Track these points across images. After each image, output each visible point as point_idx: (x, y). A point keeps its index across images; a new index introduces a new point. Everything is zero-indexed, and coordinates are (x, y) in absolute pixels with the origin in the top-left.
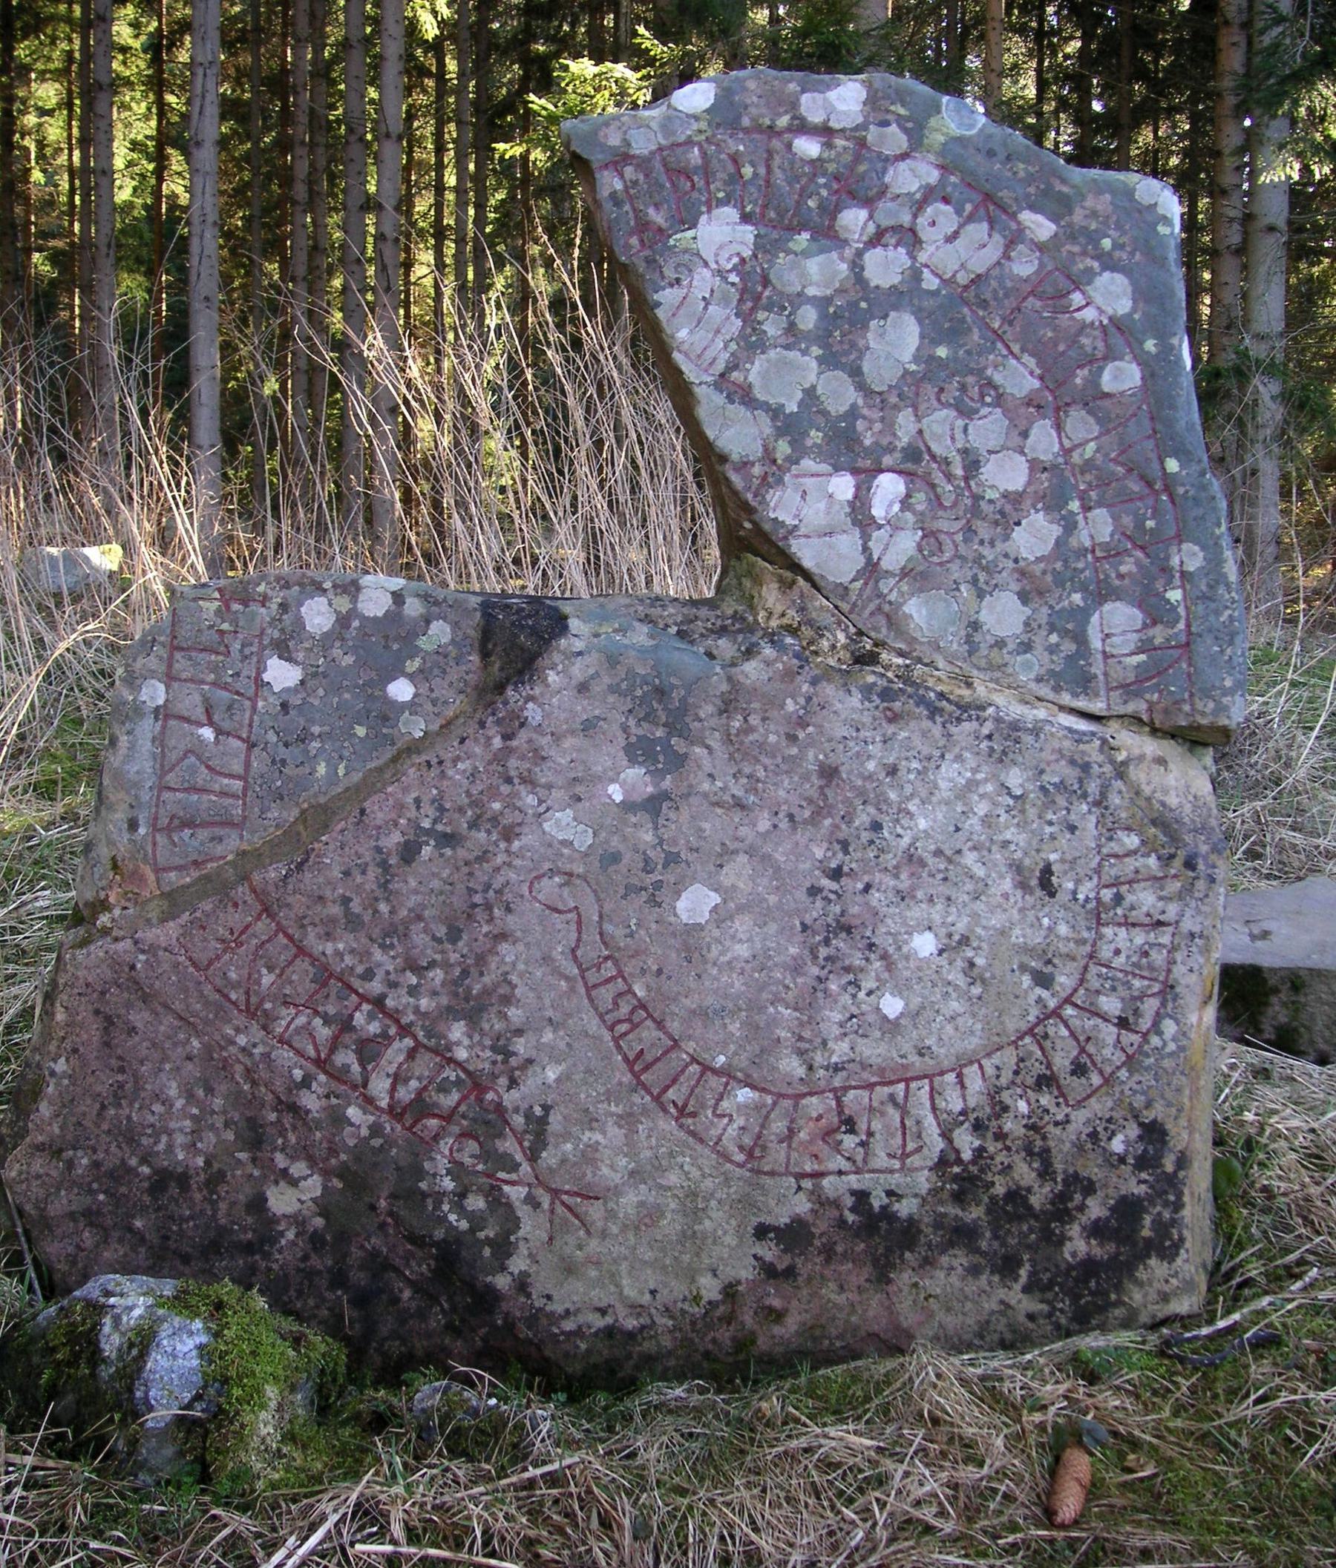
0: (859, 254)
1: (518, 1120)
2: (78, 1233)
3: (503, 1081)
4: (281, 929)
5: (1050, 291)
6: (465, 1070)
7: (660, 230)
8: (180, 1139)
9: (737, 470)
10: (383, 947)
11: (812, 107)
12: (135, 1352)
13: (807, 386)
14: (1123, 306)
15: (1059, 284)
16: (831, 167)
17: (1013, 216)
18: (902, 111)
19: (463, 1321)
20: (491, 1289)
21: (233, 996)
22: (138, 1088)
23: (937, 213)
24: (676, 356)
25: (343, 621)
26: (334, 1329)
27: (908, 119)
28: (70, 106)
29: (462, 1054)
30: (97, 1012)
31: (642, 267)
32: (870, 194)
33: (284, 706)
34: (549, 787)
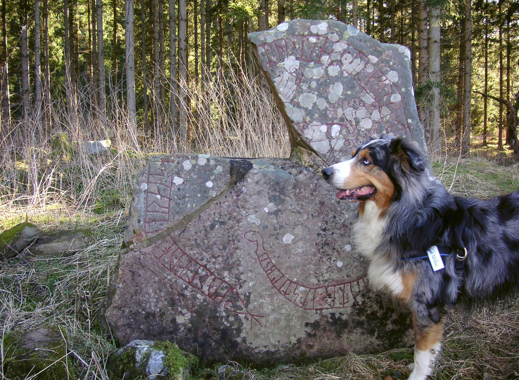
0: (327, 67)
1: (242, 297)
2: (126, 330)
3: (238, 286)
4: (179, 248)
5: (377, 76)
6: (228, 284)
7: (275, 62)
8: (153, 304)
9: (296, 125)
10: (206, 252)
11: (314, 29)
12: (145, 359)
13: (314, 102)
14: (396, 79)
15: (379, 74)
16: (319, 45)
17: (367, 57)
18: (337, 30)
19: (229, 350)
20: (236, 341)
21: (167, 266)
22: (141, 291)
23: (347, 56)
24: (280, 95)
25: (194, 166)
26: (195, 353)
27: (339, 32)
28: (89, 12)
29: (227, 280)
30: (130, 271)
31: (270, 72)
32: (329, 52)
33: (179, 189)
34: (249, 209)
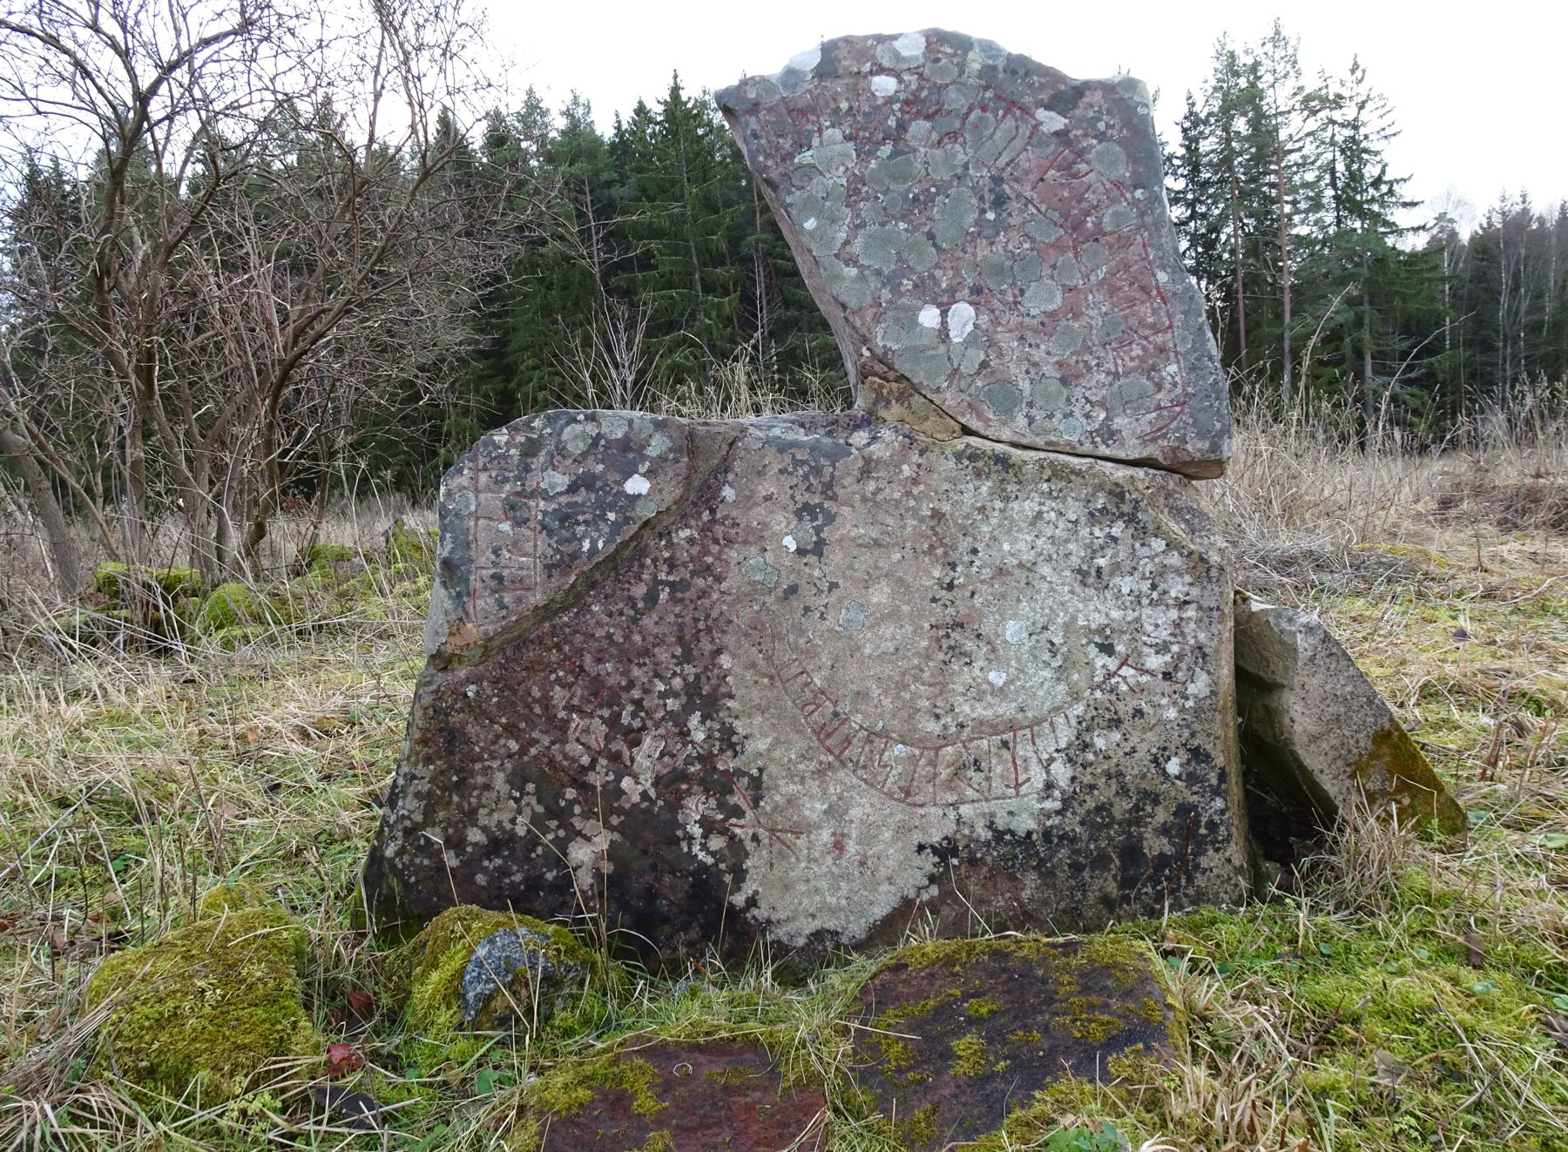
18: (949, 50)
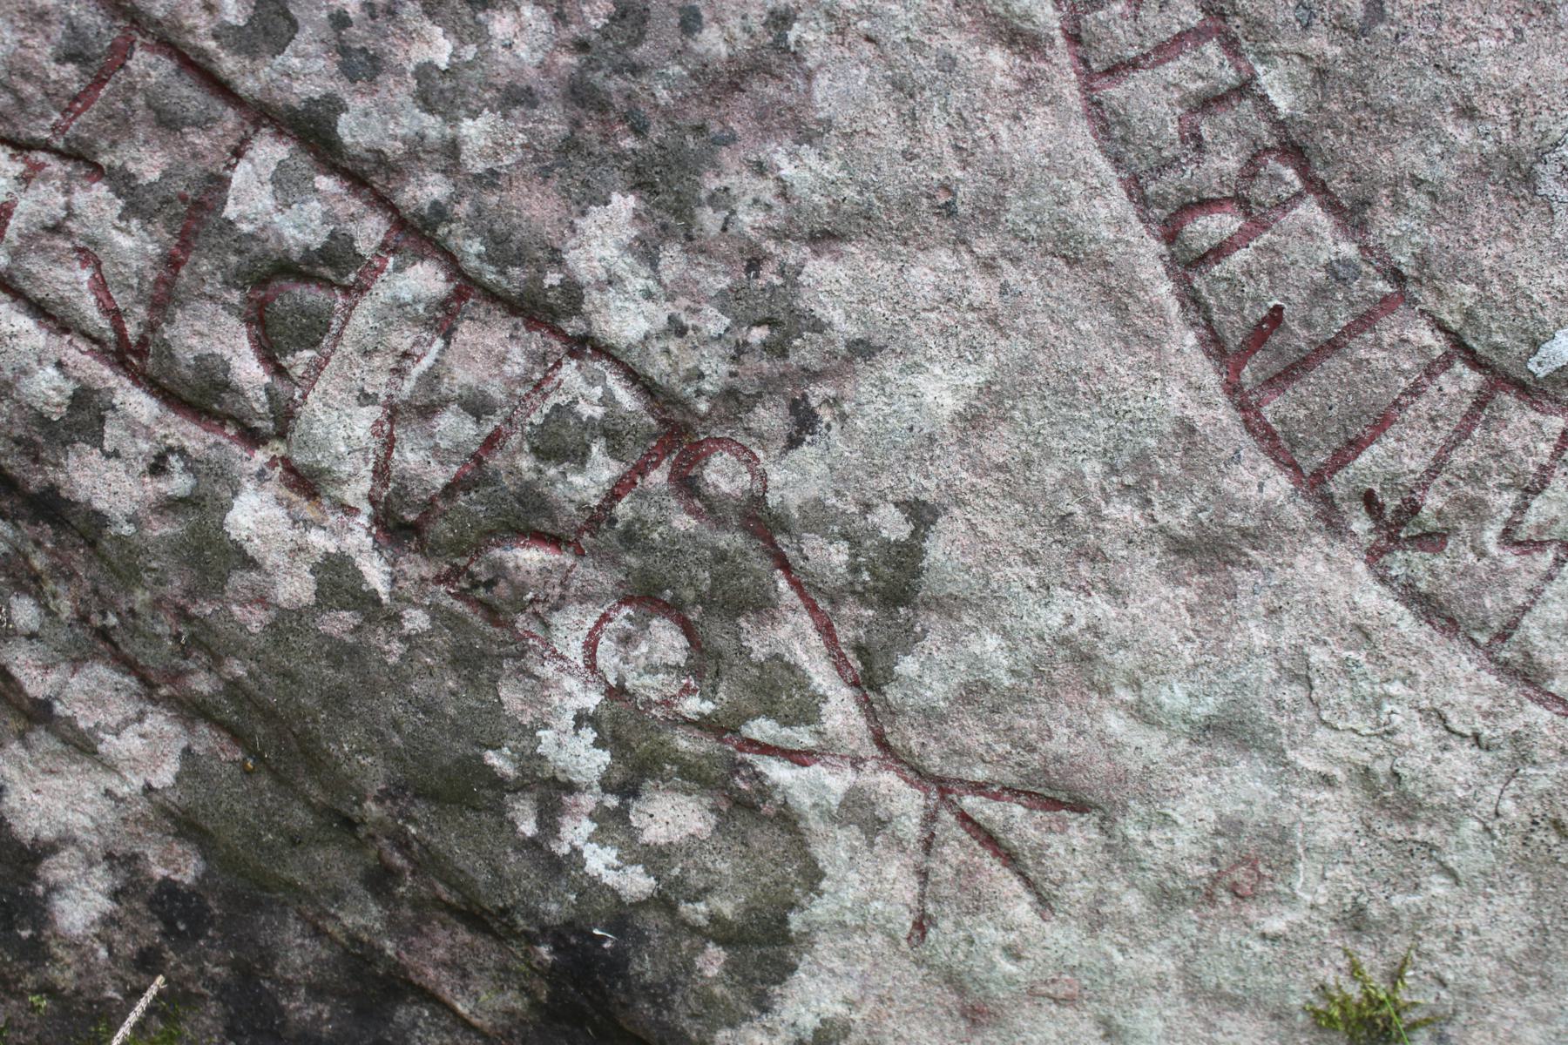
3: (770, 417)
